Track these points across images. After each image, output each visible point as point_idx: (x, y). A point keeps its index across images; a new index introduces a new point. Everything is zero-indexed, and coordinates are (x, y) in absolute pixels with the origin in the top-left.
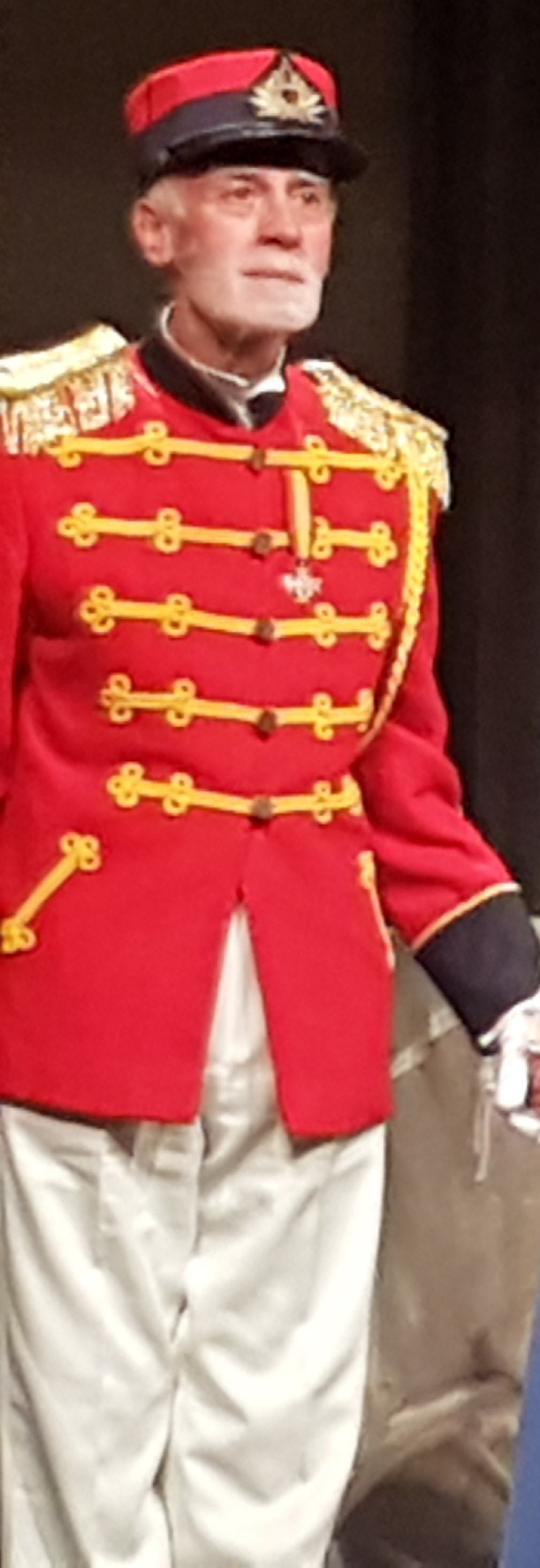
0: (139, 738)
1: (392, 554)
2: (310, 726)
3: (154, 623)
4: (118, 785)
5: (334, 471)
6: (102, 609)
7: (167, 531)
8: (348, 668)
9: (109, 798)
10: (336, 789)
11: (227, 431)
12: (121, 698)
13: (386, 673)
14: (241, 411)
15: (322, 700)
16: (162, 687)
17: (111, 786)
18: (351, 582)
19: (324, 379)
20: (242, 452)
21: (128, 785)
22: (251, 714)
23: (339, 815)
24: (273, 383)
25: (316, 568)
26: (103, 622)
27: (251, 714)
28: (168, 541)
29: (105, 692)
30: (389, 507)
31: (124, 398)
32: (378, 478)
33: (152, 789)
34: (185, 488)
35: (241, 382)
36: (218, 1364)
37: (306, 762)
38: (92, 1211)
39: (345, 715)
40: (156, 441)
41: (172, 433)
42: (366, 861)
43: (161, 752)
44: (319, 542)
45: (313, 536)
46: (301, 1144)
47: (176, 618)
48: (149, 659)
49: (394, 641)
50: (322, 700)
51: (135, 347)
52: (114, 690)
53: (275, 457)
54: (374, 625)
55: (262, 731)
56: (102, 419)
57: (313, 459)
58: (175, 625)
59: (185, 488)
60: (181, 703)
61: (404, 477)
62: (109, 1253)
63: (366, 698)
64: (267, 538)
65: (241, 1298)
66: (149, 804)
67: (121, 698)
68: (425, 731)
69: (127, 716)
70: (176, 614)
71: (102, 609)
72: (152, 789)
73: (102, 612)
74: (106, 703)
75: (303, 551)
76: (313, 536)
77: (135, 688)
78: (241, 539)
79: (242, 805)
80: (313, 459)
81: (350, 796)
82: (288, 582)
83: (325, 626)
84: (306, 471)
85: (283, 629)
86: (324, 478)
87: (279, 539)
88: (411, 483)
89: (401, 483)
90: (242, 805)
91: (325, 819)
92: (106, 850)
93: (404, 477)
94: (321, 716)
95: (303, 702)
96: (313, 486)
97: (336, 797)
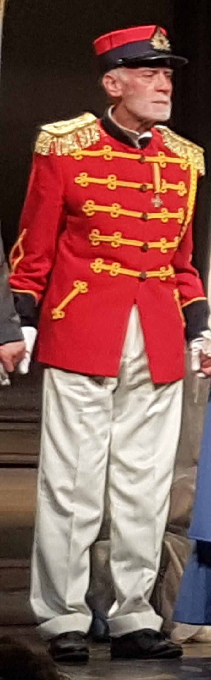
2: (160, 249)
3: (108, 213)
4: (94, 266)
6: (90, 208)
7: (112, 182)
10: (167, 269)
12: (96, 237)
15: (163, 240)
16: (111, 234)
18: (173, 201)
20: (138, 157)
21: (98, 265)
23: (168, 277)
24: (148, 135)
26: (90, 212)
27: (140, 244)
29: (91, 235)
33: (106, 267)
35: (137, 133)
41: (113, 150)
44: (163, 187)
45: (161, 186)
47: (115, 211)
48: (106, 225)
50: (163, 240)
52: (93, 234)
53: (148, 159)
55: (143, 249)
58: (115, 214)
60: (116, 240)
64: (145, 186)
67: (96, 237)
70: (115, 210)
71: (90, 208)
72: (106, 267)
73: (90, 209)
74: (91, 238)
75: (158, 190)
76: (161, 186)
77: (101, 234)
80: (161, 159)
81: (171, 271)
83: (164, 215)
85: (151, 216)
86: (164, 166)
87: (150, 186)
91: (164, 279)
94: (163, 245)
96: (161, 169)
97: (167, 271)
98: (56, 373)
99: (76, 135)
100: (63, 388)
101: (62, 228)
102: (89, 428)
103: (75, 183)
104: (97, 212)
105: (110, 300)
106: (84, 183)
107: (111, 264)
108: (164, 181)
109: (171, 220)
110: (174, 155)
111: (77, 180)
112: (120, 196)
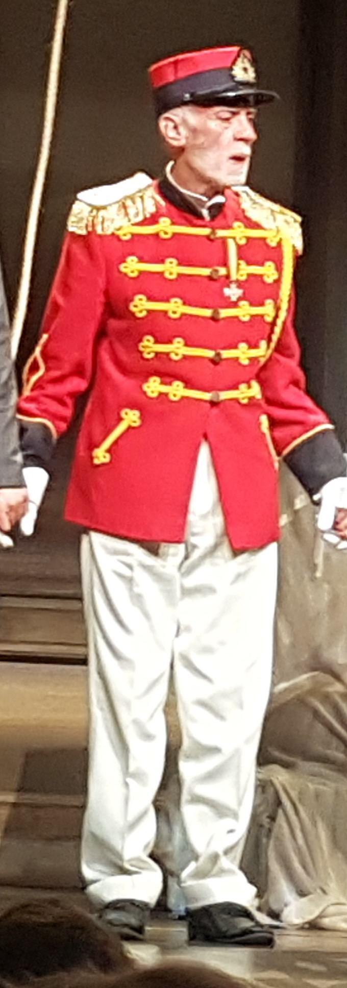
0: (157, 364)
1: (276, 276)
3: (165, 313)
5: (249, 239)
6: (141, 306)
7: (171, 268)
8: (255, 331)
9: (145, 393)
10: (249, 387)
11: (200, 222)
12: (149, 347)
13: (272, 332)
14: (205, 213)
15: (243, 346)
16: (170, 342)
17: (145, 387)
18: (256, 291)
19: (243, 195)
20: (206, 231)
21: (153, 387)
22: (210, 354)
23: (251, 399)
24: (219, 199)
25: (240, 285)
26: (141, 312)
27: (210, 354)
28: (171, 274)
29: (141, 344)
30: (275, 254)
31: (151, 209)
32: (268, 241)
33: (164, 389)
35: (205, 199)
39: (254, 353)
40: (166, 227)
41: (173, 223)
42: (264, 419)
43: (167, 371)
44: (241, 272)
47: (175, 309)
49: (276, 317)
50: (243, 346)
51: (155, 182)
52: (145, 343)
53: (221, 233)
54: (267, 310)
55: (215, 362)
56: (140, 218)
57: (238, 233)
58: (174, 312)
60: (178, 349)
61: (281, 240)
63: (263, 344)
64: (217, 271)
66: (163, 396)
67: (149, 347)
68: (290, 356)
69: (152, 355)
70: (175, 307)
71: (141, 306)
72: (164, 389)
73: (141, 308)
74: (141, 349)
75: (234, 276)
76: (238, 269)
78: (206, 272)
79: (207, 396)
80: (238, 233)
81: (255, 391)
82: (227, 291)
83: (245, 311)
84: (234, 238)
85: (224, 313)
86: (243, 242)
87: (222, 271)
88: (284, 243)
89: (279, 244)
90: (207, 396)
91: (245, 401)
92: (142, 417)
93: (281, 240)
94: (243, 353)
95: (235, 347)
96: (239, 247)
97: (250, 391)
98: (96, 537)
100: (106, 557)
101: (101, 333)
103: (120, 272)
104: (150, 312)
106: (132, 272)
107: (170, 384)
108: (242, 263)
109: (253, 317)
110: (257, 226)
111: (123, 268)
112: (180, 287)
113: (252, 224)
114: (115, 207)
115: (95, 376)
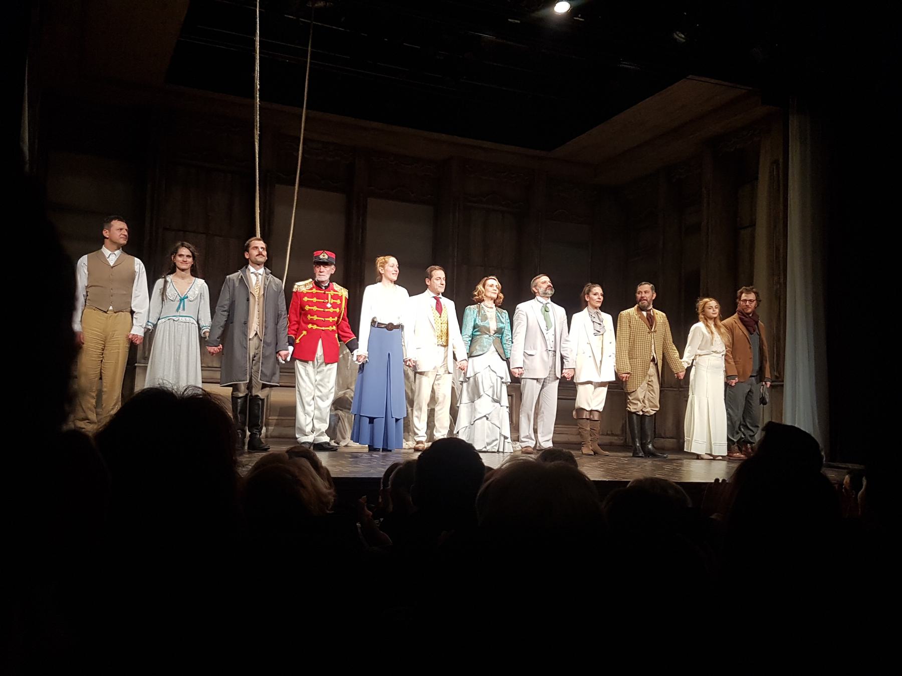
6: (307, 308)
7: (315, 300)
8: (333, 315)
12: (309, 317)
21: (310, 326)
30: (341, 298)
34: (317, 296)
36: (320, 387)
37: (329, 324)
38: (306, 370)
40: (314, 291)
46: (327, 364)
48: (312, 313)
54: (338, 310)
57: (332, 293)
59: (317, 296)
60: (315, 318)
62: (308, 375)
65: (321, 380)
67: (309, 317)
70: (315, 308)
71: (307, 308)
80: (332, 293)
81: (334, 328)
83: (332, 310)
94: (331, 319)
99: (305, 285)
102: (308, 375)
105: (313, 337)
112: (317, 304)
113: (335, 291)
114: (303, 286)
115: (298, 323)
